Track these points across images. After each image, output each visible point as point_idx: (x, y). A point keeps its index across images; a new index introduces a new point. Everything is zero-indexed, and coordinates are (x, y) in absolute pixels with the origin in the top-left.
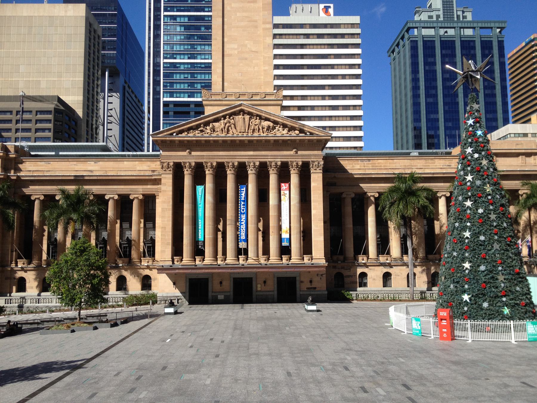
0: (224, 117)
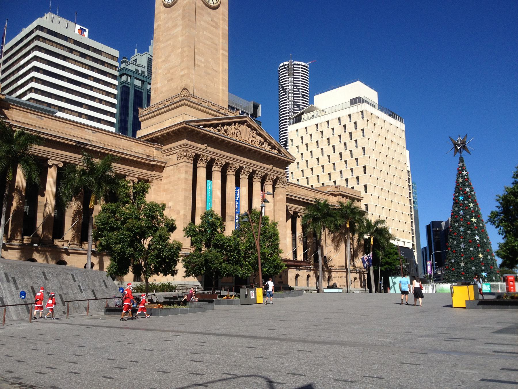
0: (235, 123)
